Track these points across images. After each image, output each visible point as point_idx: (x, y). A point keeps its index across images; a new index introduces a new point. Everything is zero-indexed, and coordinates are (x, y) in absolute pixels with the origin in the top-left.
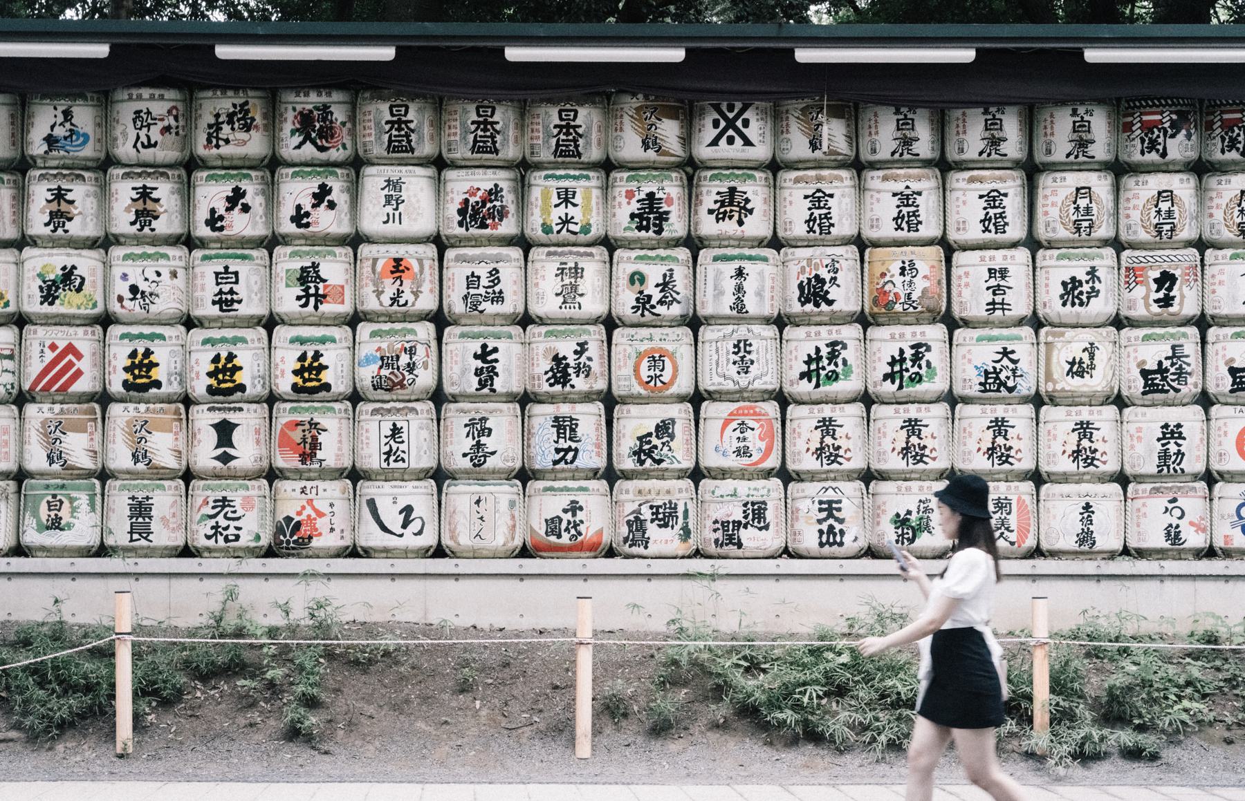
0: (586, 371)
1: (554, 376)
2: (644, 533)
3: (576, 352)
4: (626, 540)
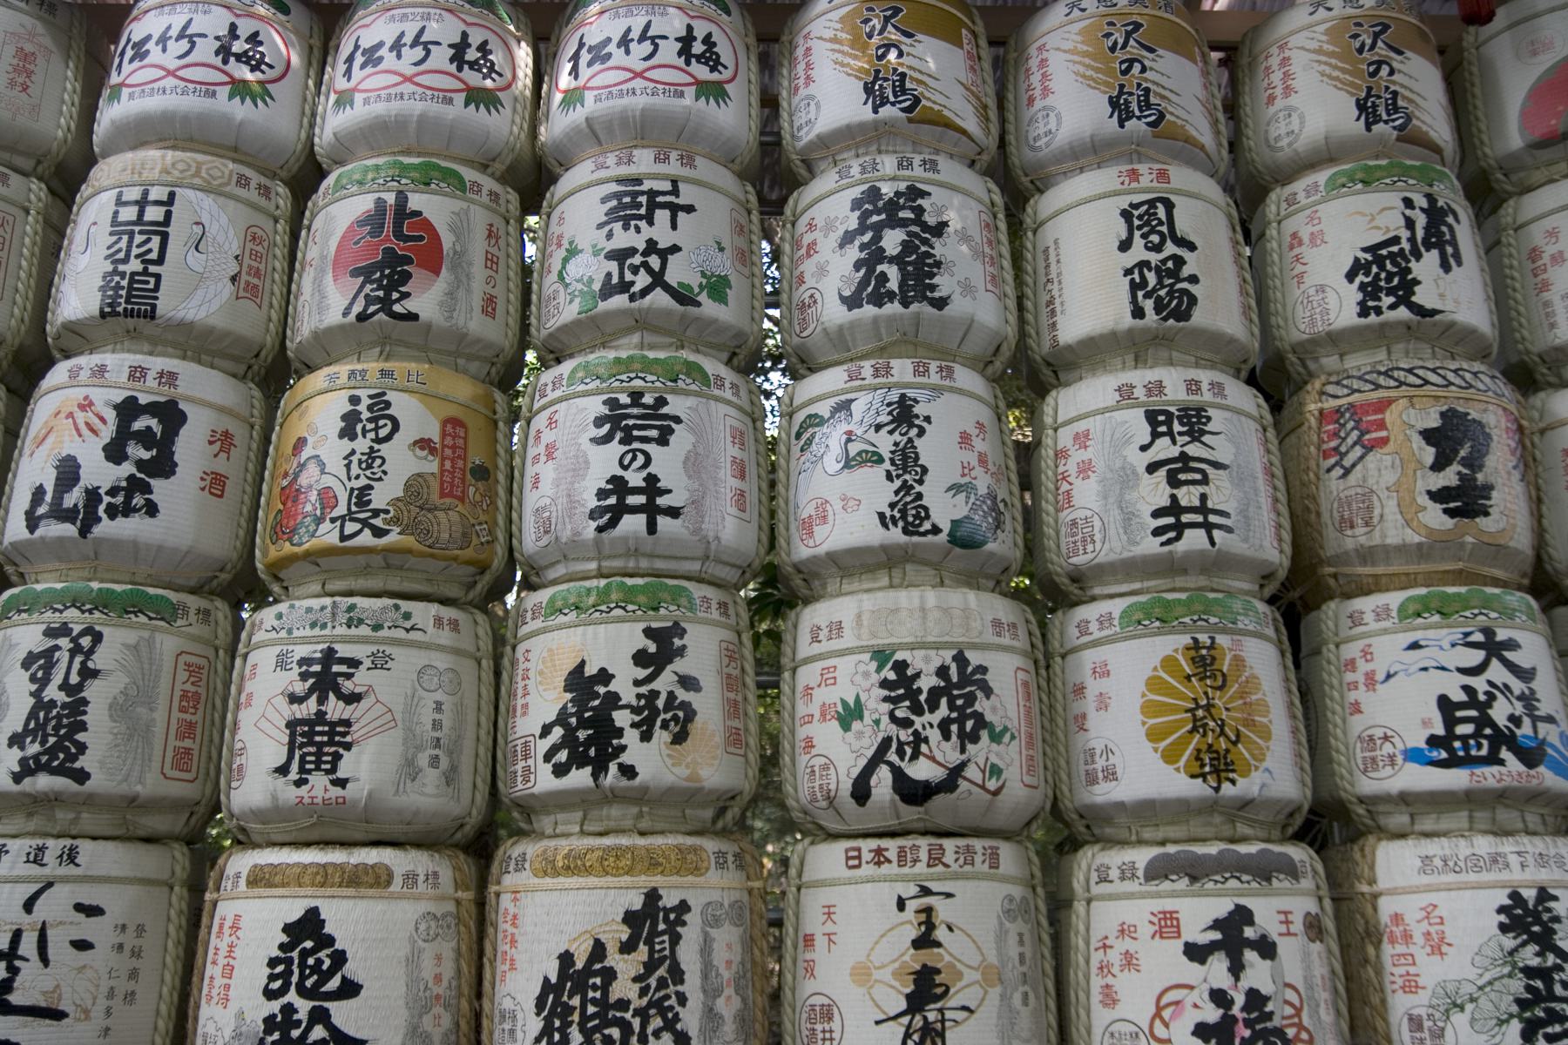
0: (669, 718)
1: (569, 740)
3: (640, 658)
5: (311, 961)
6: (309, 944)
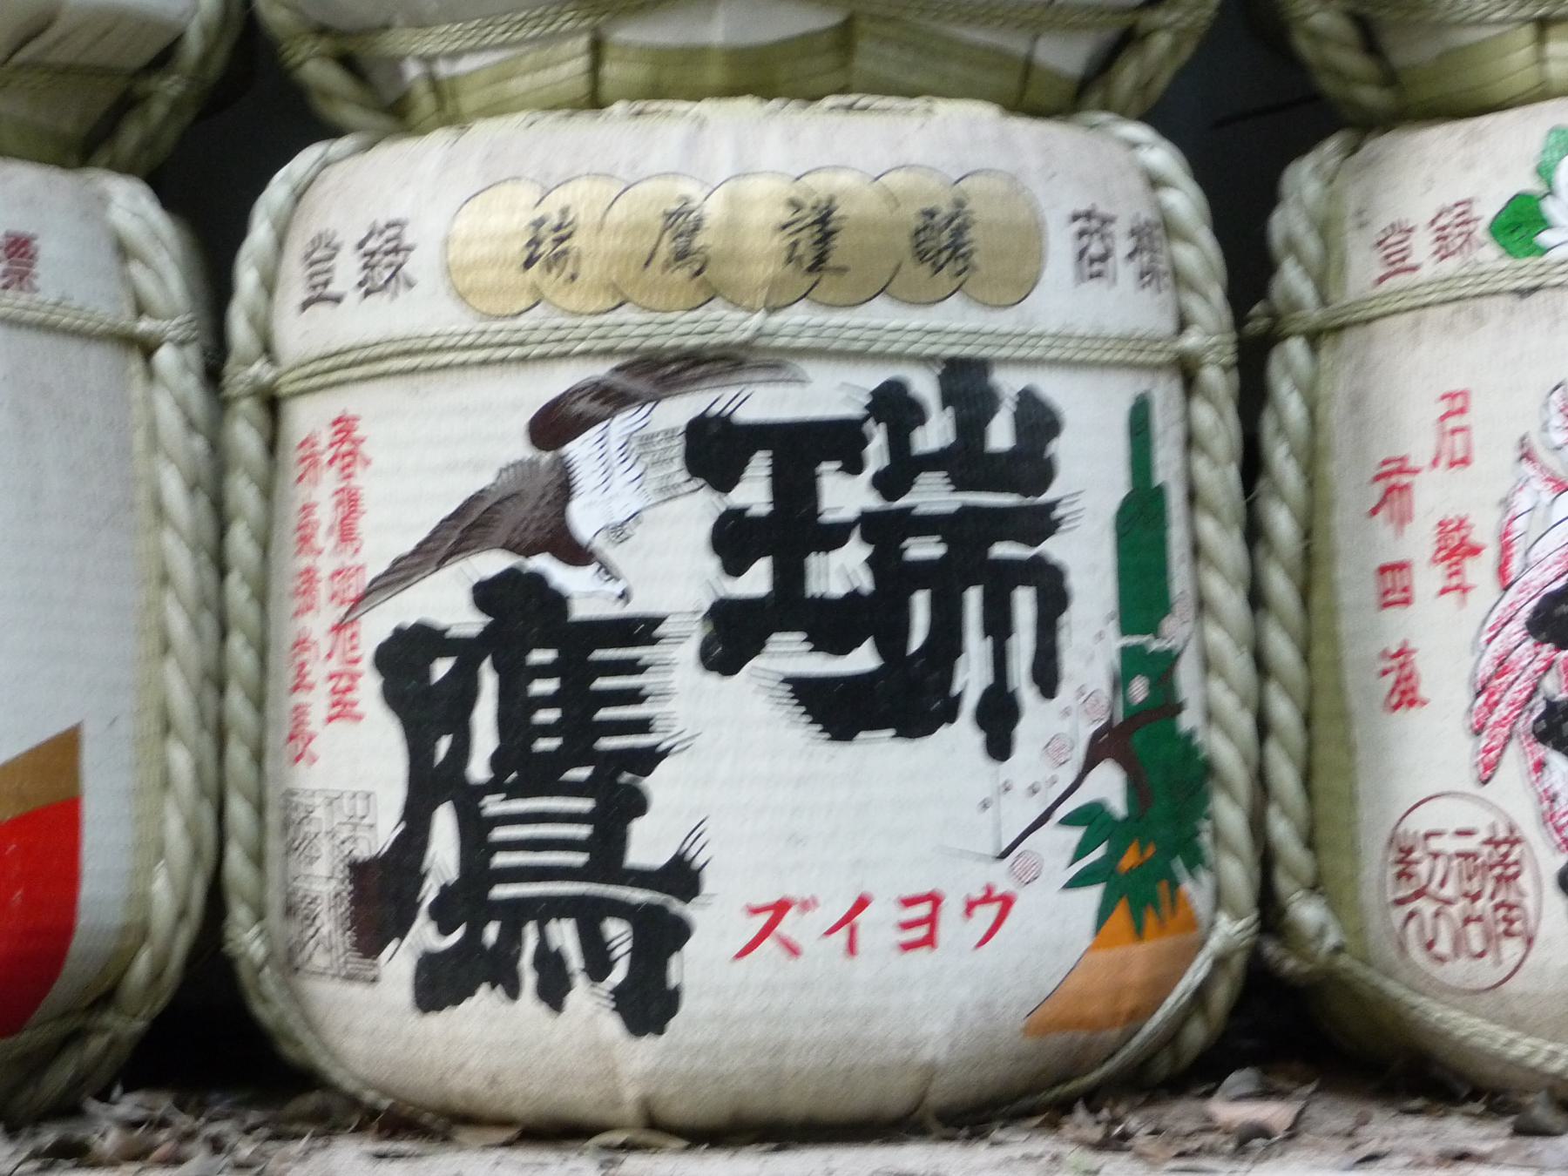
2: (619, 805)
4: (381, 895)
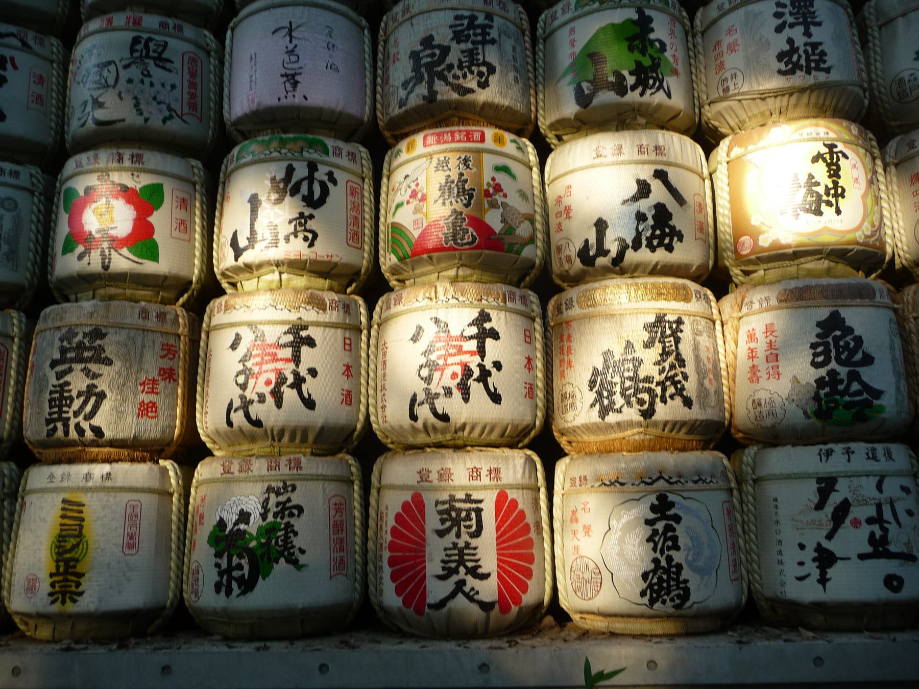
5: (842, 343)
6: (838, 333)
